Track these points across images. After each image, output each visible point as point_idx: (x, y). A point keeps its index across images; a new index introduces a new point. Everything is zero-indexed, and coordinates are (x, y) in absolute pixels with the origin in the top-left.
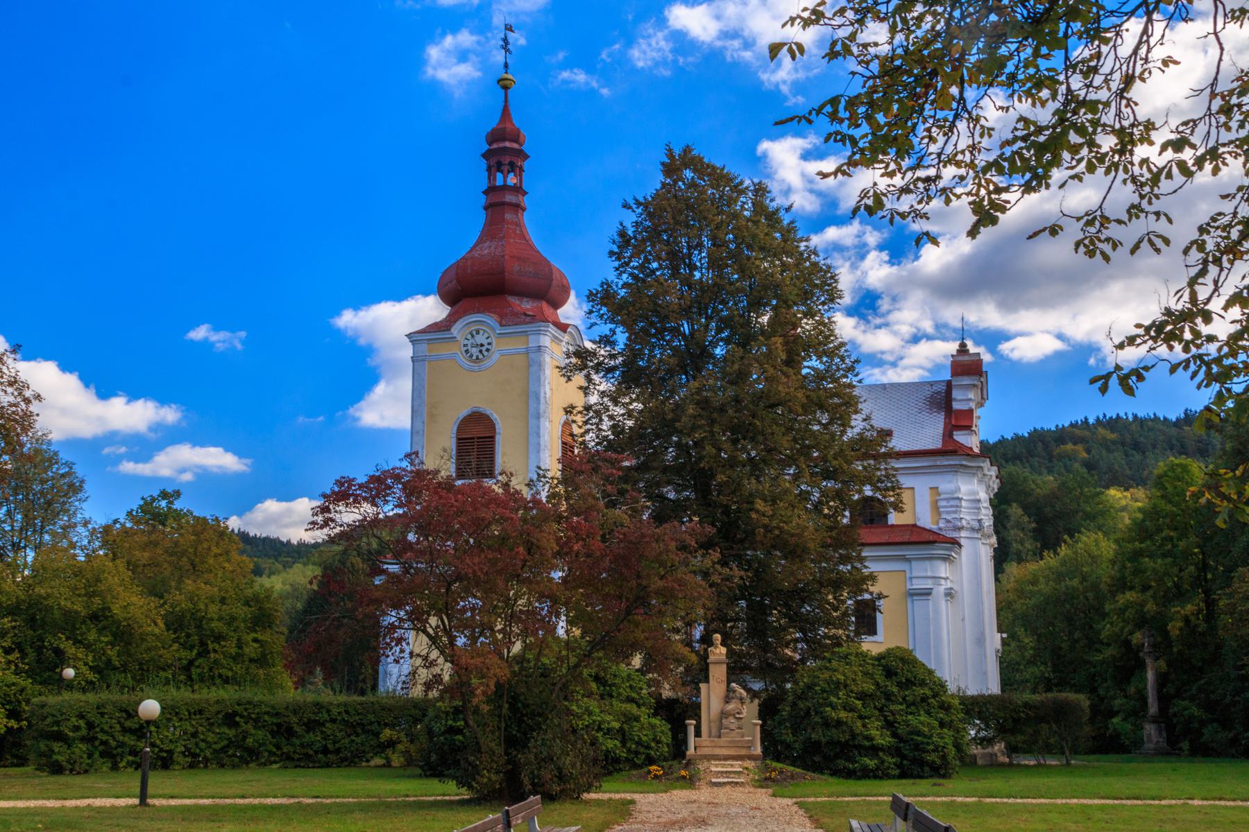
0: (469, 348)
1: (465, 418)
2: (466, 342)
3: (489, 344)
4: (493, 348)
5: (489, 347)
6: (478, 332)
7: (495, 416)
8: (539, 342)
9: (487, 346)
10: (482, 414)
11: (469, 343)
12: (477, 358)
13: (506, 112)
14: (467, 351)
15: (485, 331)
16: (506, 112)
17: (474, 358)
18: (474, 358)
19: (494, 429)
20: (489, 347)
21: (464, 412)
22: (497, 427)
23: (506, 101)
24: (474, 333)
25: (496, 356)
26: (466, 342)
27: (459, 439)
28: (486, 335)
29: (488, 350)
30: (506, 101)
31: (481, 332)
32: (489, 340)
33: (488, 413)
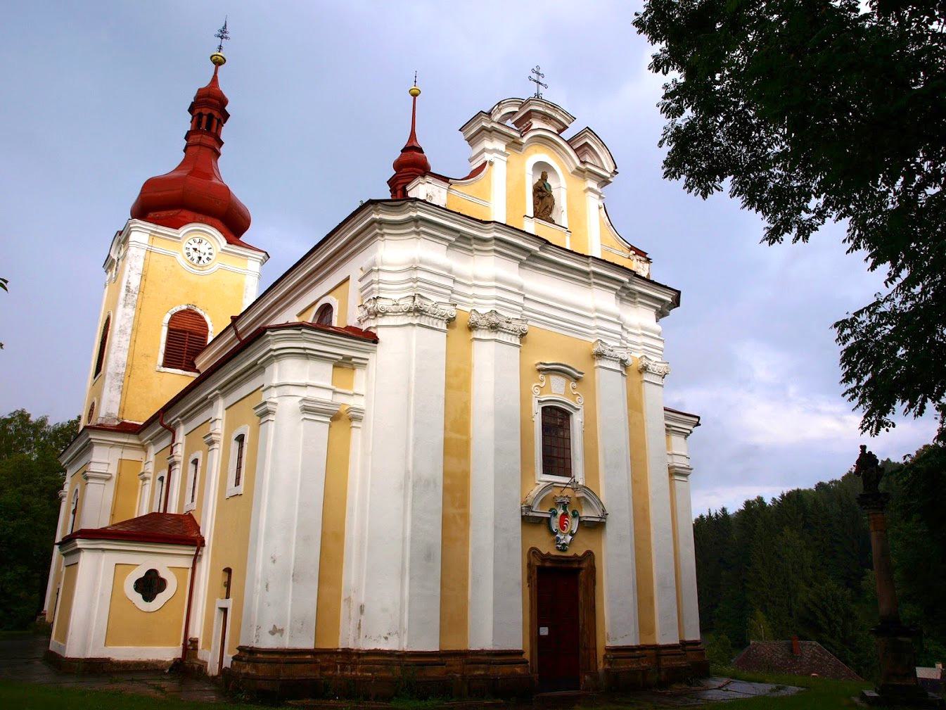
2: (188, 246)
3: (210, 254)
9: (207, 255)
11: (191, 247)
13: (215, 79)
14: (188, 254)
16: (215, 79)
20: (210, 257)
23: (216, 73)
24: (197, 240)
26: (188, 246)
27: (170, 330)
29: (208, 259)
30: (216, 73)
31: (204, 242)
32: (210, 251)
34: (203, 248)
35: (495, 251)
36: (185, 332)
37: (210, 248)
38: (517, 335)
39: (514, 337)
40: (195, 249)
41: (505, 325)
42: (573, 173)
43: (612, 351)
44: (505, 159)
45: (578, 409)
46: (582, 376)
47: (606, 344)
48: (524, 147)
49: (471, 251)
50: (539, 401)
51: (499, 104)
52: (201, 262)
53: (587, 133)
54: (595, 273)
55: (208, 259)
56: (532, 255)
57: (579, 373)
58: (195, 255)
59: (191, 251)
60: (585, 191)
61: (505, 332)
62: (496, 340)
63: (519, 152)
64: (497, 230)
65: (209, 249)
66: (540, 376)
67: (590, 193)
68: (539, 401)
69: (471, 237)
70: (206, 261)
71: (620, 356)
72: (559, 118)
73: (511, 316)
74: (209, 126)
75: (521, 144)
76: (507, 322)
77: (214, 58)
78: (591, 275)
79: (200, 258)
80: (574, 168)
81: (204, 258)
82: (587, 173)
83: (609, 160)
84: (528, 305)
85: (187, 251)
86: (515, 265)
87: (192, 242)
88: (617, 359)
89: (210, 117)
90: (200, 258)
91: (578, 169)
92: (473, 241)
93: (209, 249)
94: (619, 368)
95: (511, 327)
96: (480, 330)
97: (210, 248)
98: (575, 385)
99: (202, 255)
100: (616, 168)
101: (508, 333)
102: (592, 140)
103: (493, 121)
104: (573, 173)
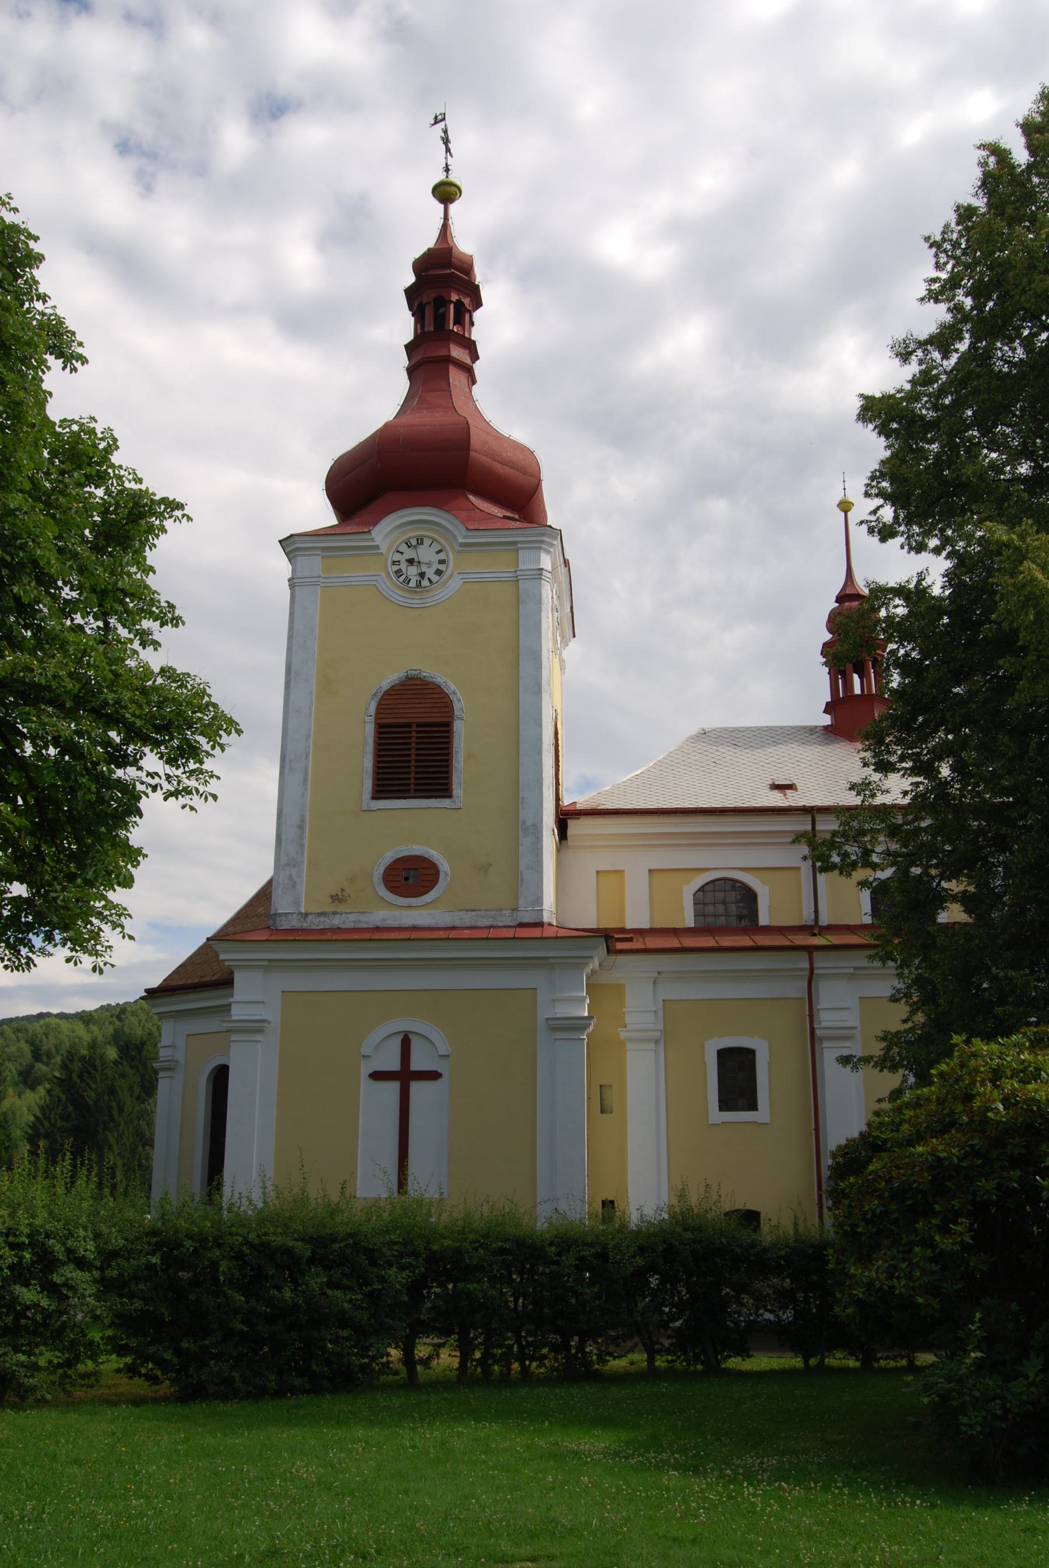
0: (403, 566)
1: (392, 688)
3: (442, 562)
4: (449, 569)
5: (442, 567)
6: (420, 541)
7: (451, 687)
8: (538, 562)
9: (436, 566)
10: (428, 683)
12: (419, 585)
14: (399, 573)
15: (434, 540)
17: (413, 584)
18: (413, 584)
19: (451, 711)
20: (442, 567)
21: (390, 678)
22: (456, 706)
25: (455, 584)
26: (397, 557)
28: (436, 547)
29: (439, 572)
31: (427, 542)
32: (442, 556)
33: (440, 679)
34: (426, 554)
36: (409, 725)
37: (440, 551)
40: (411, 562)
52: (425, 583)
55: (439, 572)
58: (413, 571)
59: (403, 566)
65: (439, 552)
70: (435, 578)
74: (441, 320)
77: (442, 188)
79: (422, 575)
81: (430, 573)
85: (396, 568)
87: (403, 548)
89: (441, 302)
90: (422, 575)
93: (439, 552)
97: (440, 551)
99: (424, 568)
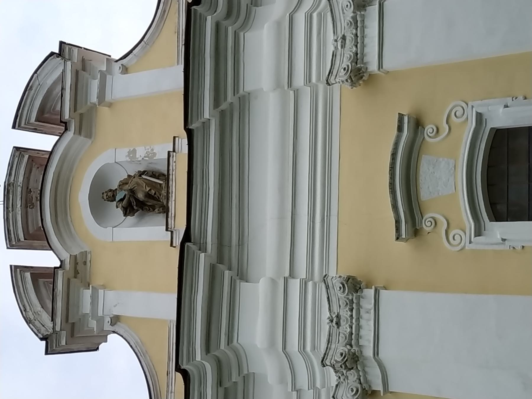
35: (229, 341)
38: (358, 298)
39: (363, 302)
41: (345, 328)
42: (89, 136)
43: (344, 38)
44: (101, 292)
45: (479, 116)
46: (406, 119)
47: (334, 55)
48: (76, 252)
49: (245, 379)
50: (478, 233)
51: (28, 321)
53: (23, 125)
54: (216, 102)
56: (220, 259)
57: (400, 129)
60: (110, 105)
61: (359, 327)
62: (376, 352)
63: (89, 256)
64: (191, 356)
66: (427, 226)
67: (108, 98)
68: (478, 233)
69: (221, 391)
71: (350, 13)
72: (21, 179)
73: (326, 314)
75: (75, 259)
76: (338, 324)
78: (224, 106)
80: (82, 138)
82: (79, 111)
83: (46, 71)
84: (302, 271)
86: (244, 287)
88: (359, 19)
91: (79, 131)
92: (227, 384)
94: (377, 6)
95: (345, 314)
96: (369, 378)
98: (429, 129)
100: (52, 54)
101: (358, 319)
102: (30, 111)
103: (54, 328)
104: (89, 136)
